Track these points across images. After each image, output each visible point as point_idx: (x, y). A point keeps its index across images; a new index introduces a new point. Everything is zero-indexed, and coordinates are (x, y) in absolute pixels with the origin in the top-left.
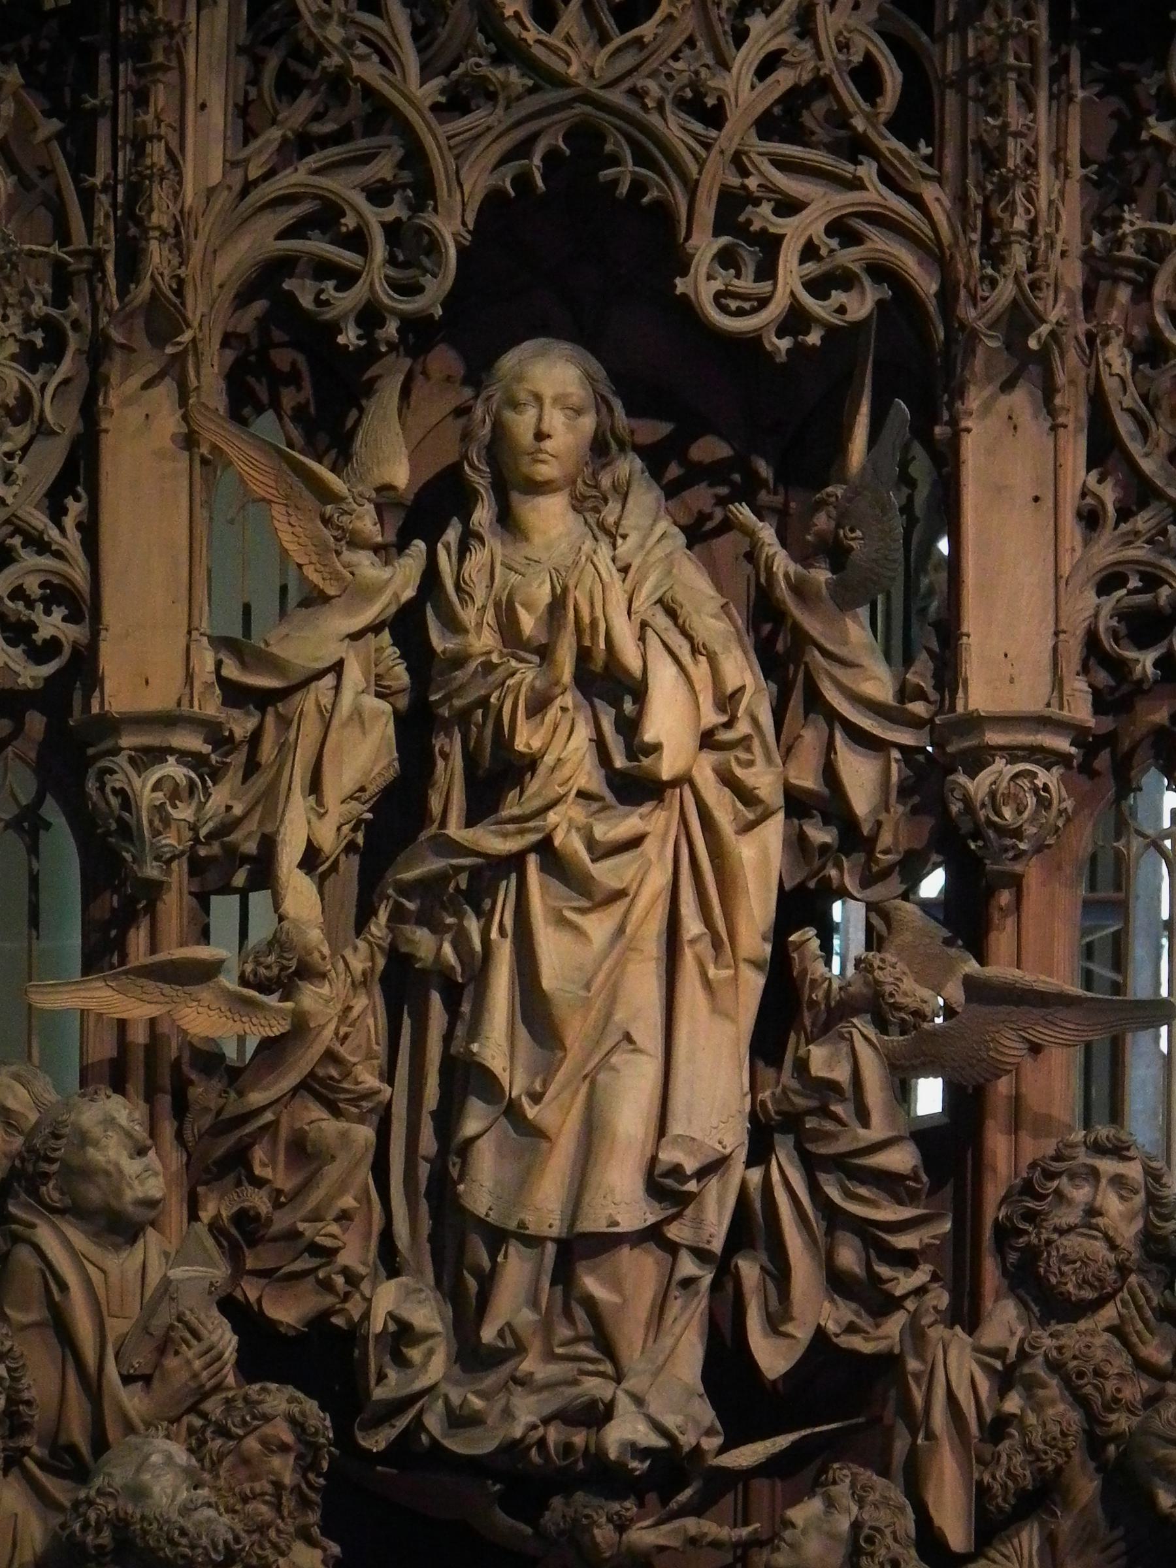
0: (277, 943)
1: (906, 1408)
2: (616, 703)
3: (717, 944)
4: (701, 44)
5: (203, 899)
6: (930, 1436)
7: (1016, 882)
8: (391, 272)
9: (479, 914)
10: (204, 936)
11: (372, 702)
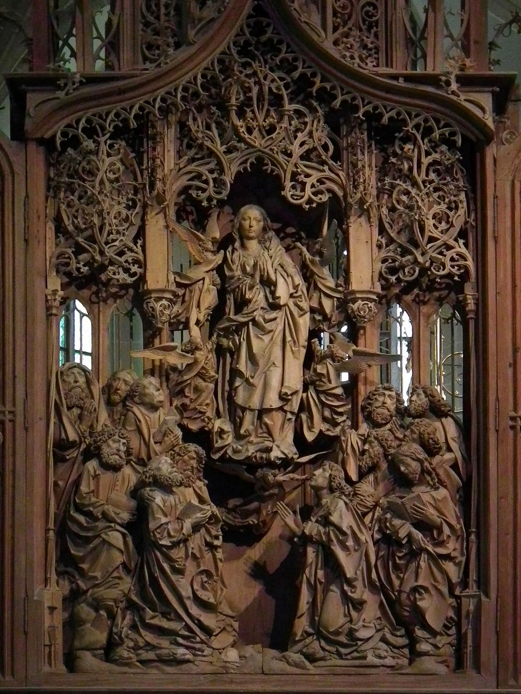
0: (190, 342)
1: (342, 446)
2: (270, 287)
3: (294, 342)
4: (286, 139)
5: (172, 332)
6: (347, 454)
7: (364, 328)
8: (215, 189)
9: (238, 335)
10: (173, 340)
11: (212, 287)
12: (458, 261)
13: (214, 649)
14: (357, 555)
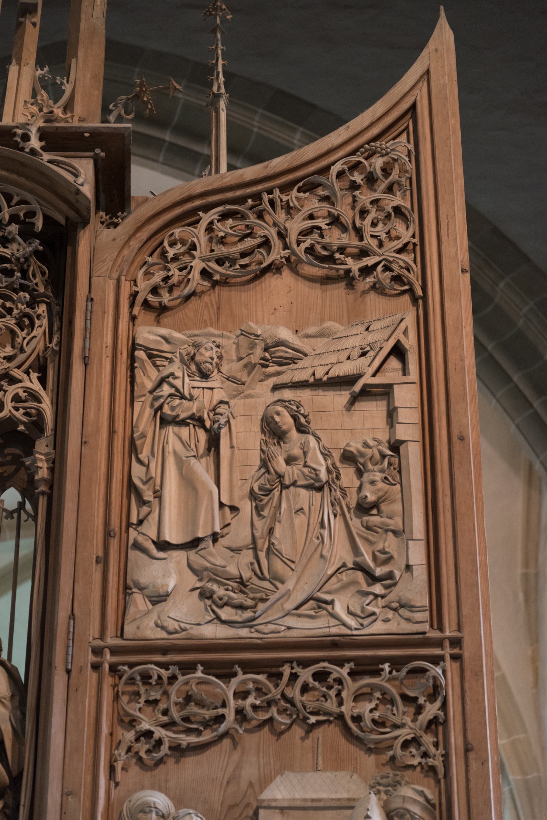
12: (26, 401)
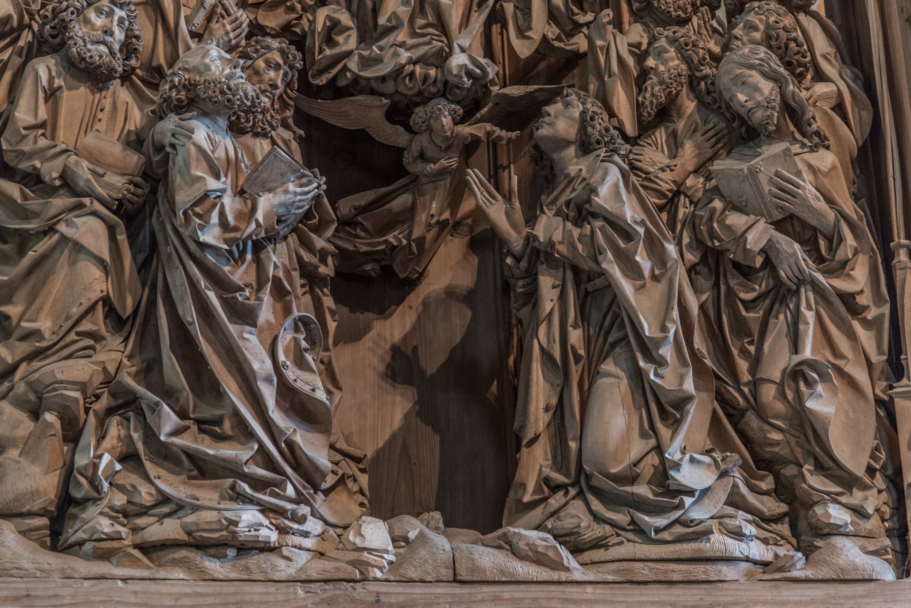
13: (326, 522)
14: (657, 290)
